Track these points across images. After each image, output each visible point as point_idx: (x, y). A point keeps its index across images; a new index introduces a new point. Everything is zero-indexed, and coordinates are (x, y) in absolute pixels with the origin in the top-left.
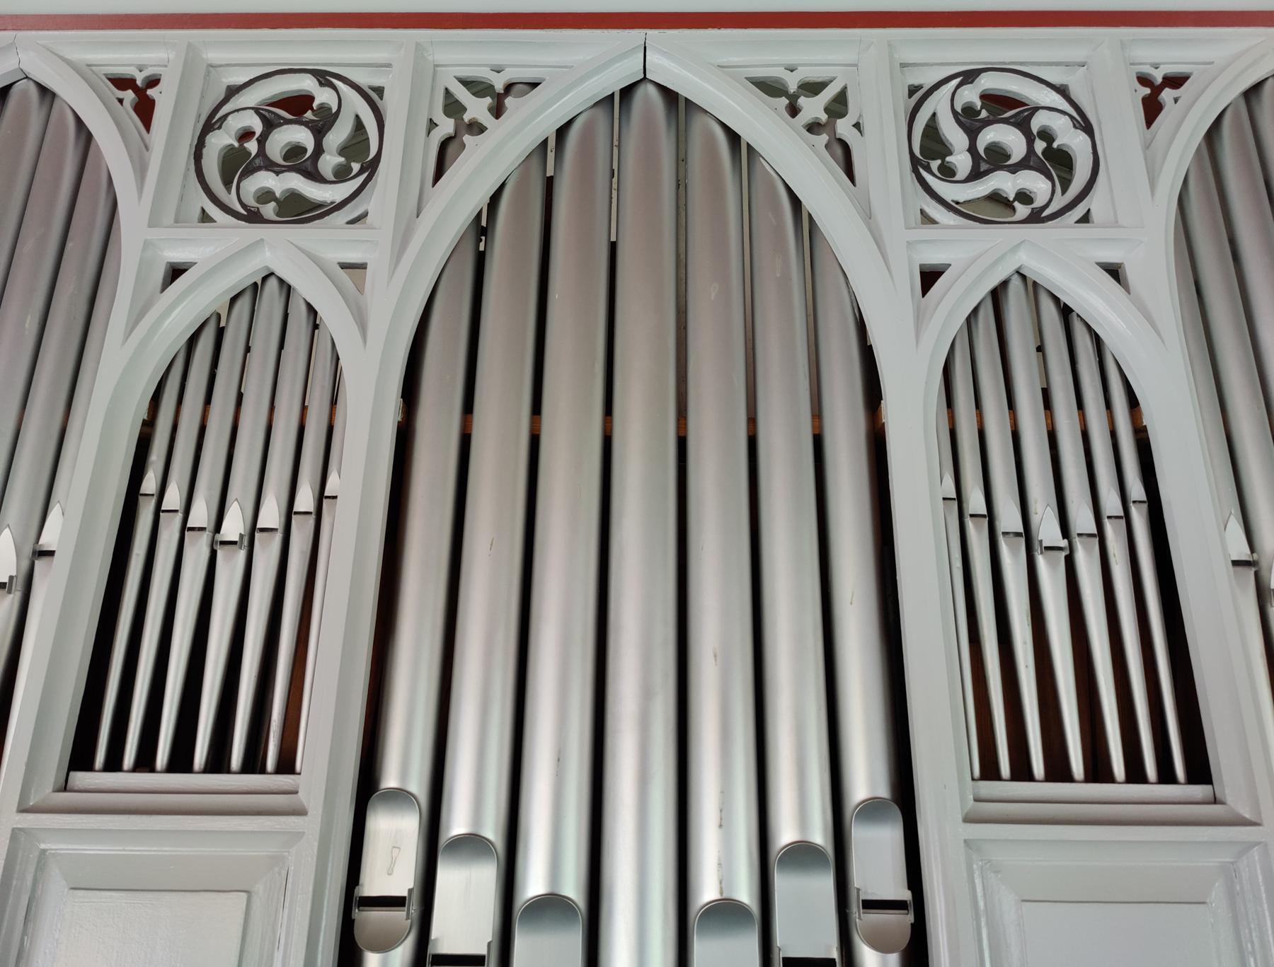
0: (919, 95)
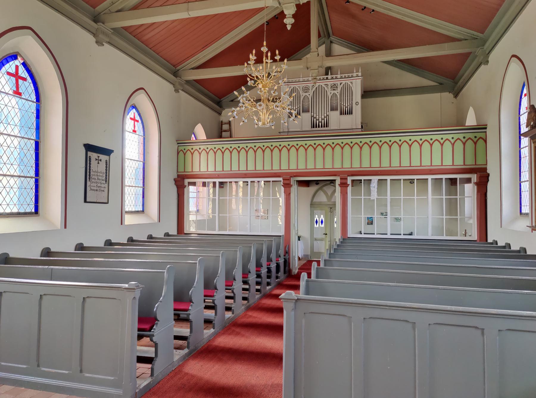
0: (331, 84)
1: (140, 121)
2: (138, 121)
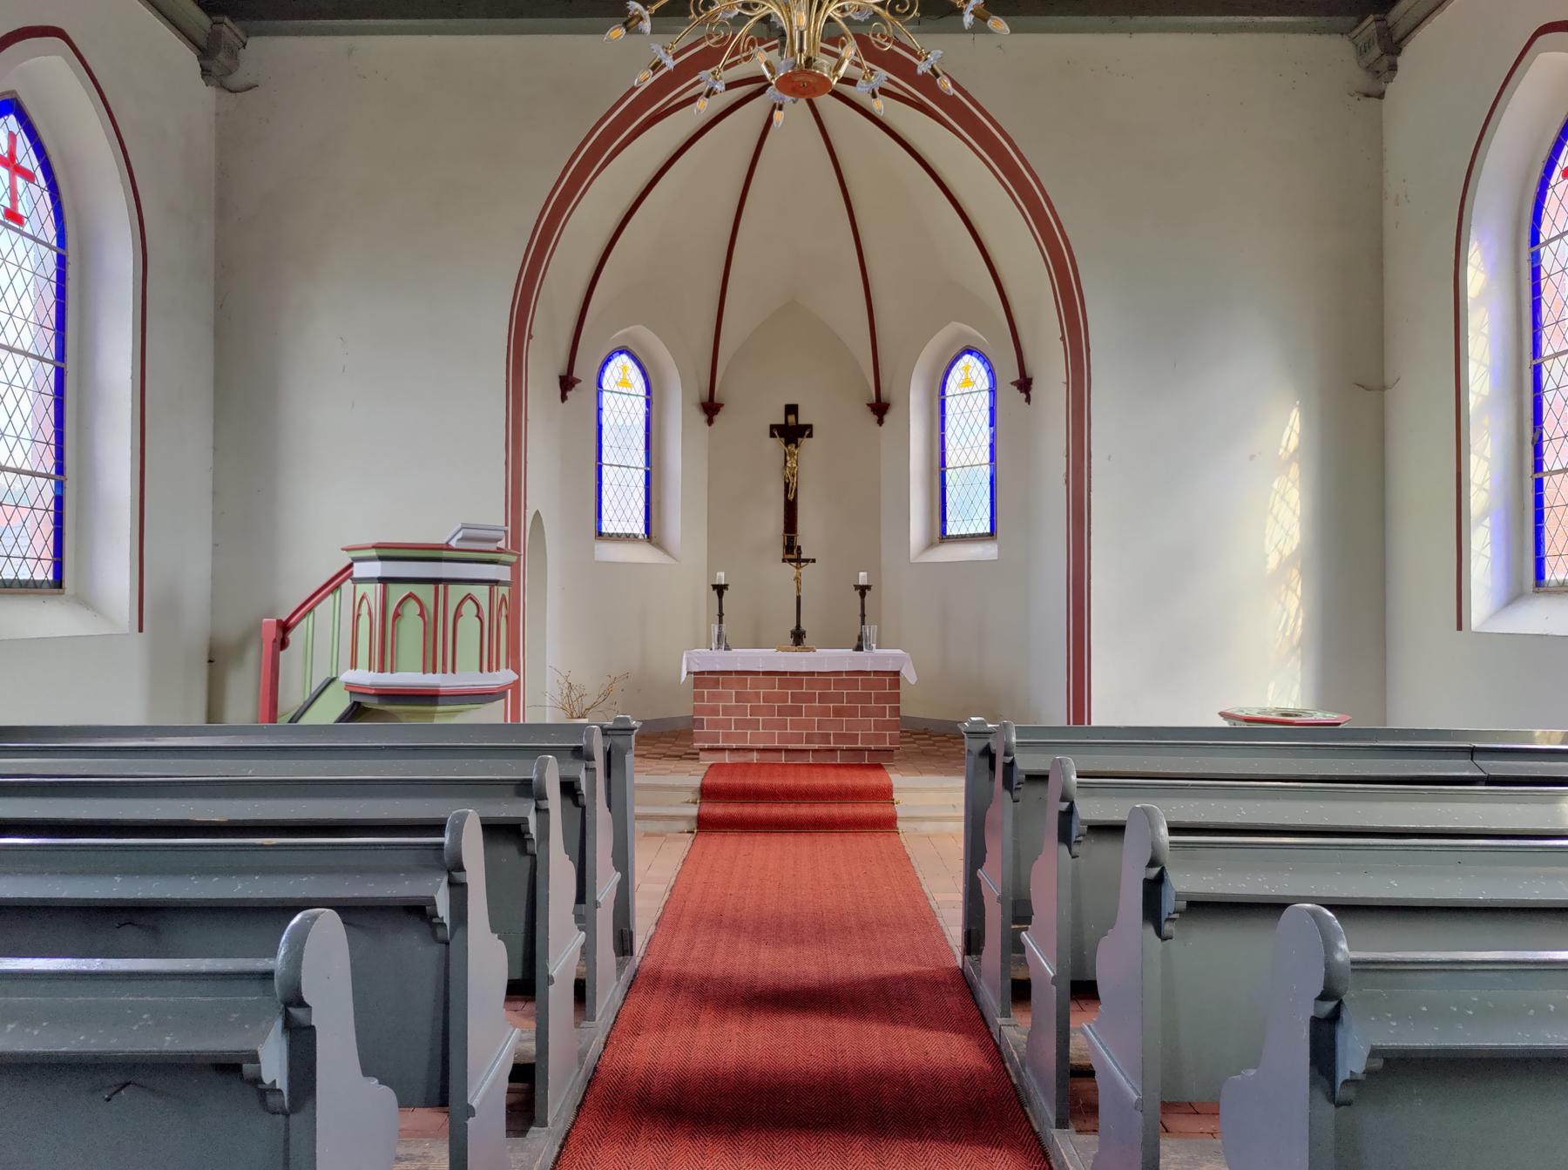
1: (39, 174)
2: (29, 176)
